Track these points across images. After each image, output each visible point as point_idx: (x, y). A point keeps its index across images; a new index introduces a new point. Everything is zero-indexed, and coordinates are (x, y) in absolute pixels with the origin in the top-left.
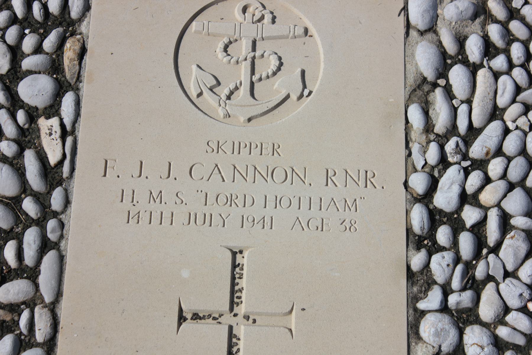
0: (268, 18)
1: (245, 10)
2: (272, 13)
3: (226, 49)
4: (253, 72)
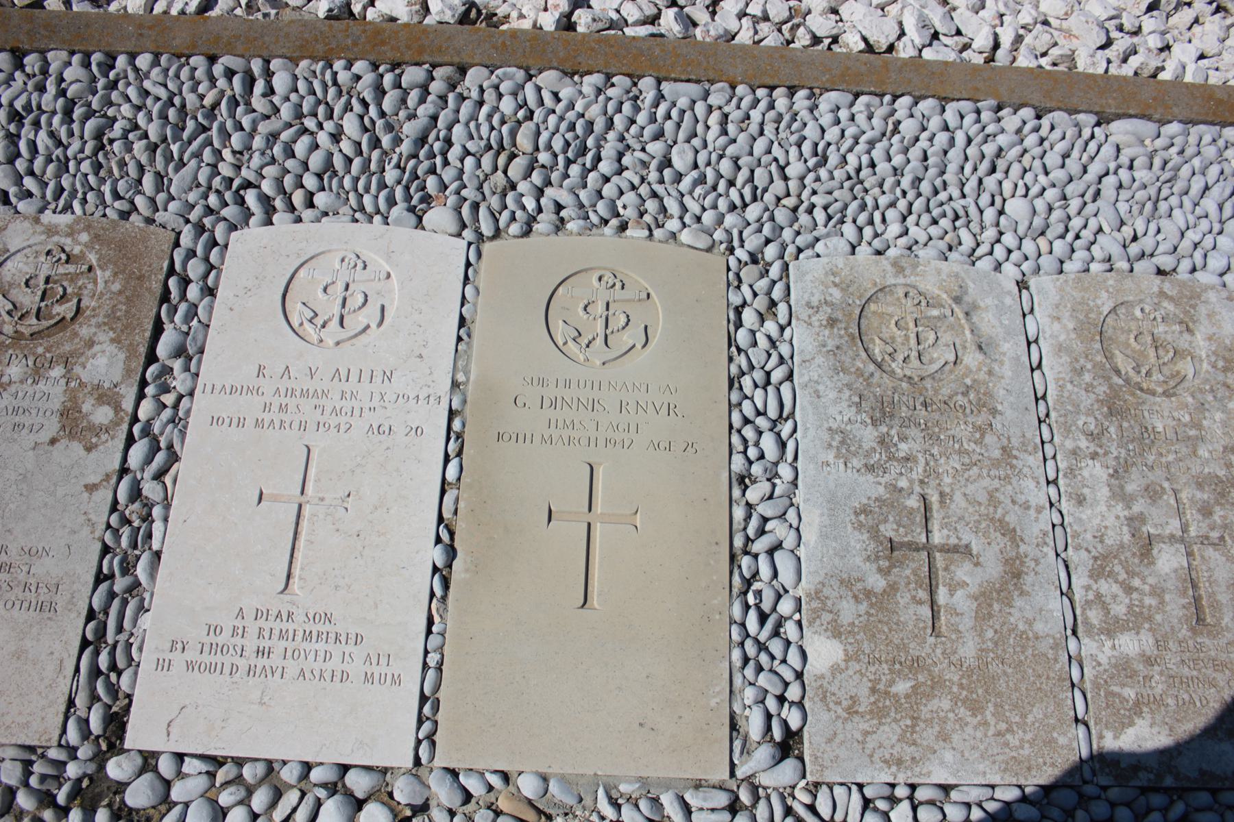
0: (618, 285)
1: (600, 279)
3: (585, 309)
4: (607, 327)
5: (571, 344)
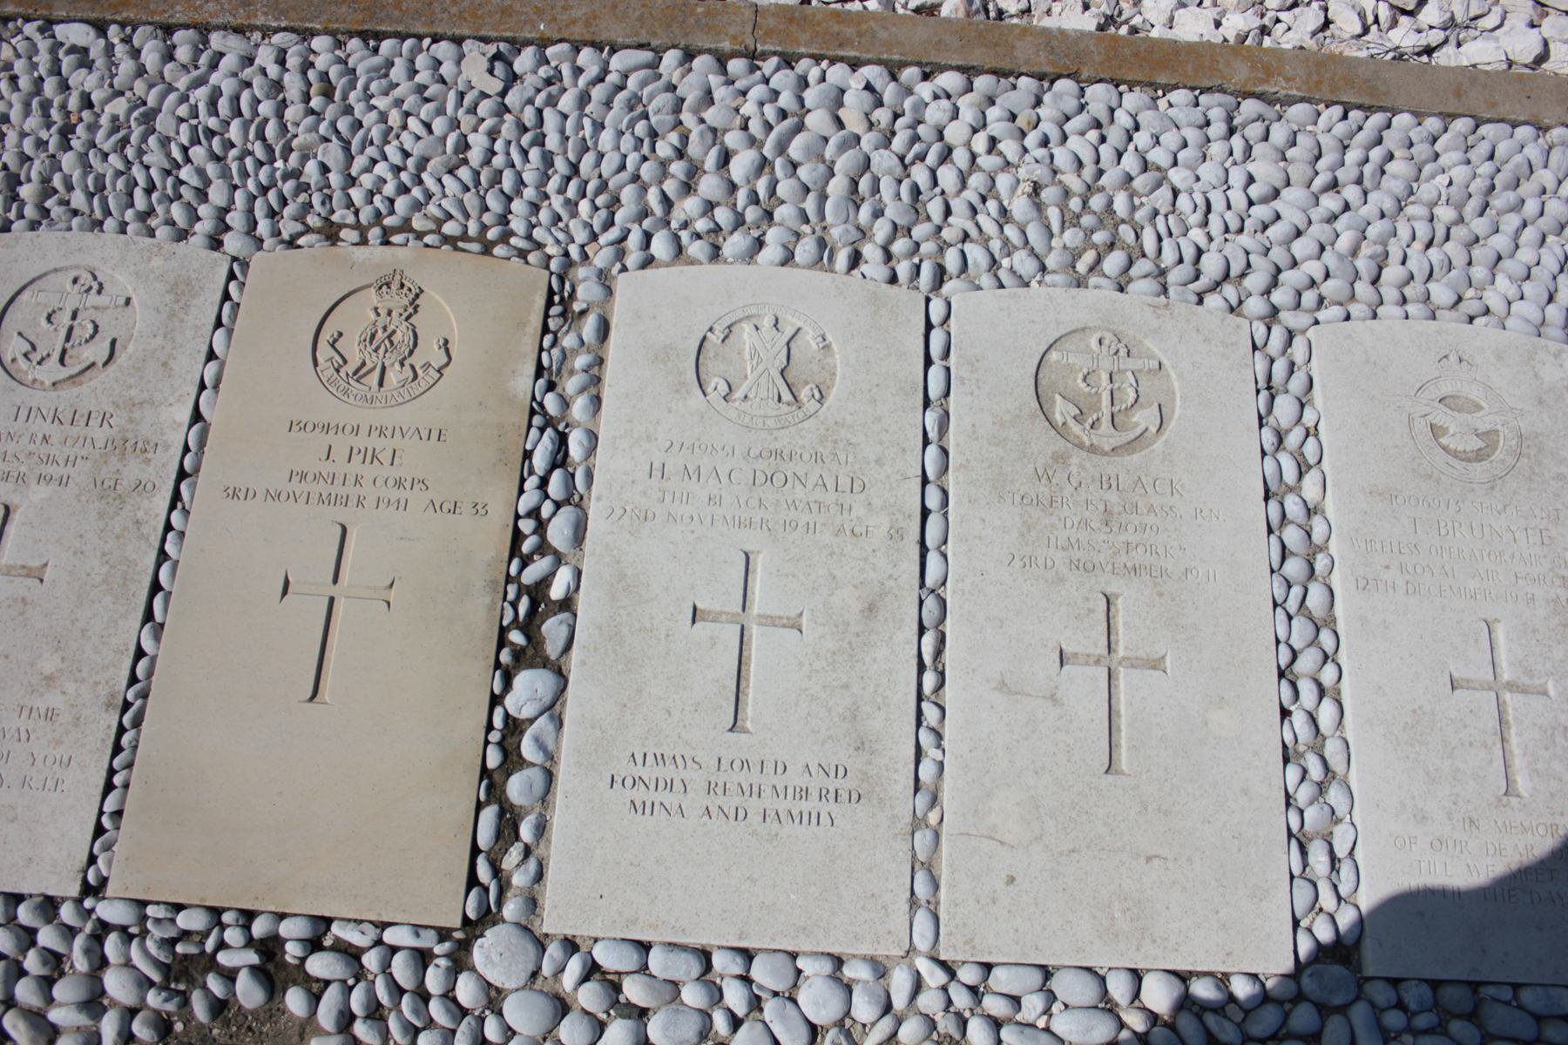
0: (96, 287)
2: (101, 285)
5: (22, 363)
